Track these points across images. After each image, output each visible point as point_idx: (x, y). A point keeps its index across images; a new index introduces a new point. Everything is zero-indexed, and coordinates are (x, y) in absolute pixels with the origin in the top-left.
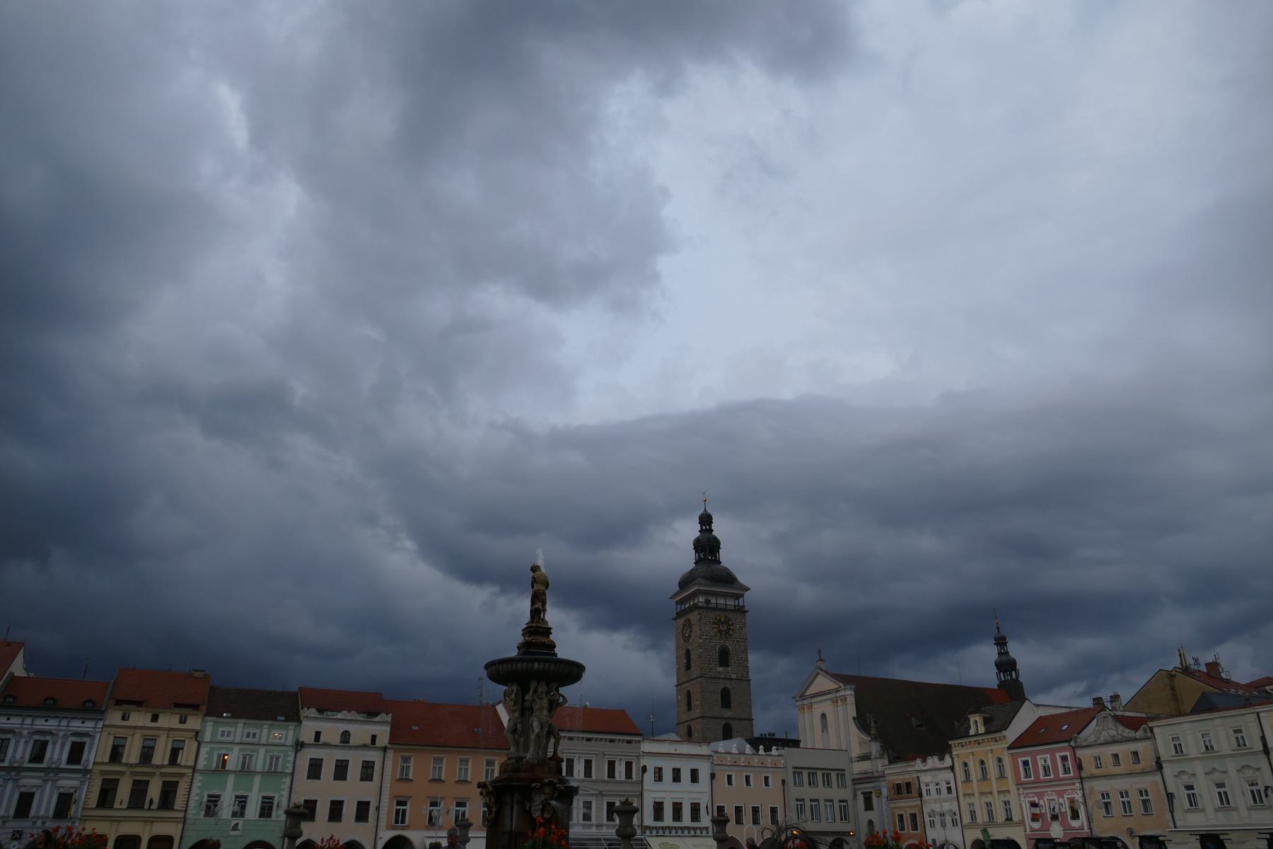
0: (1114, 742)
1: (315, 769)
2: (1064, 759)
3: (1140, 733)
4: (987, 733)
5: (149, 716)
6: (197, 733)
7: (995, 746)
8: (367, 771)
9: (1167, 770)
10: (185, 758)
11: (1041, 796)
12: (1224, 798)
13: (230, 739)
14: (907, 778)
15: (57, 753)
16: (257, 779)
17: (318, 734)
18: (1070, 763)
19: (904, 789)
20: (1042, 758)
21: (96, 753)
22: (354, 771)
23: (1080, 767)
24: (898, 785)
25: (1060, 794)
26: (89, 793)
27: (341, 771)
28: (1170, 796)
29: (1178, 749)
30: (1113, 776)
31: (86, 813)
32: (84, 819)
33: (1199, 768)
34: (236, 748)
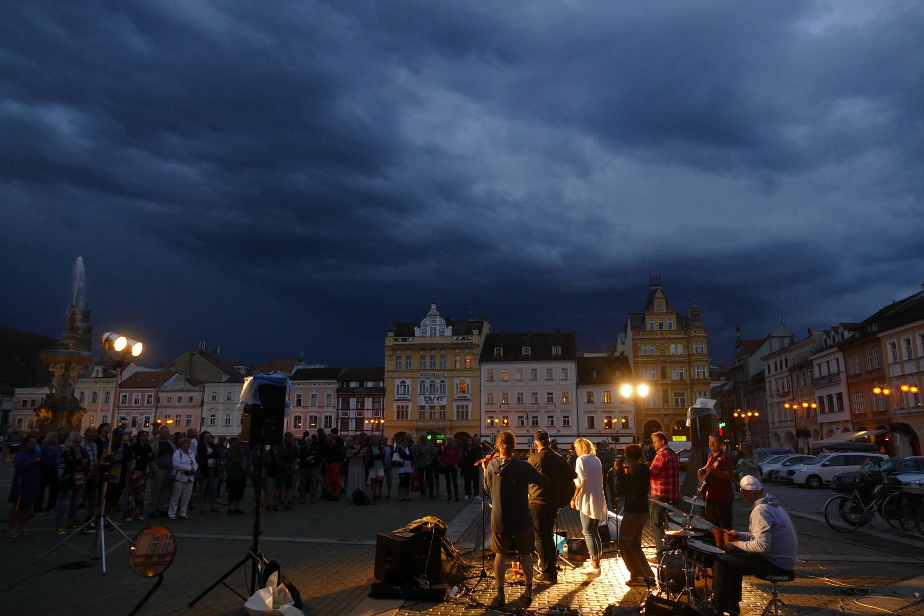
0: (182, 391)
2: (150, 396)
3: (197, 388)
4: (103, 377)
7: (106, 385)
9: (205, 407)
11: (128, 414)
12: (228, 421)
14: (33, 397)
18: (152, 399)
19: (29, 405)
20: (136, 394)
23: (158, 401)
24: (25, 402)
25: (141, 414)
28: (203, 419)
29: (214, 398)
30: (176, 407)
33: (221, 407)
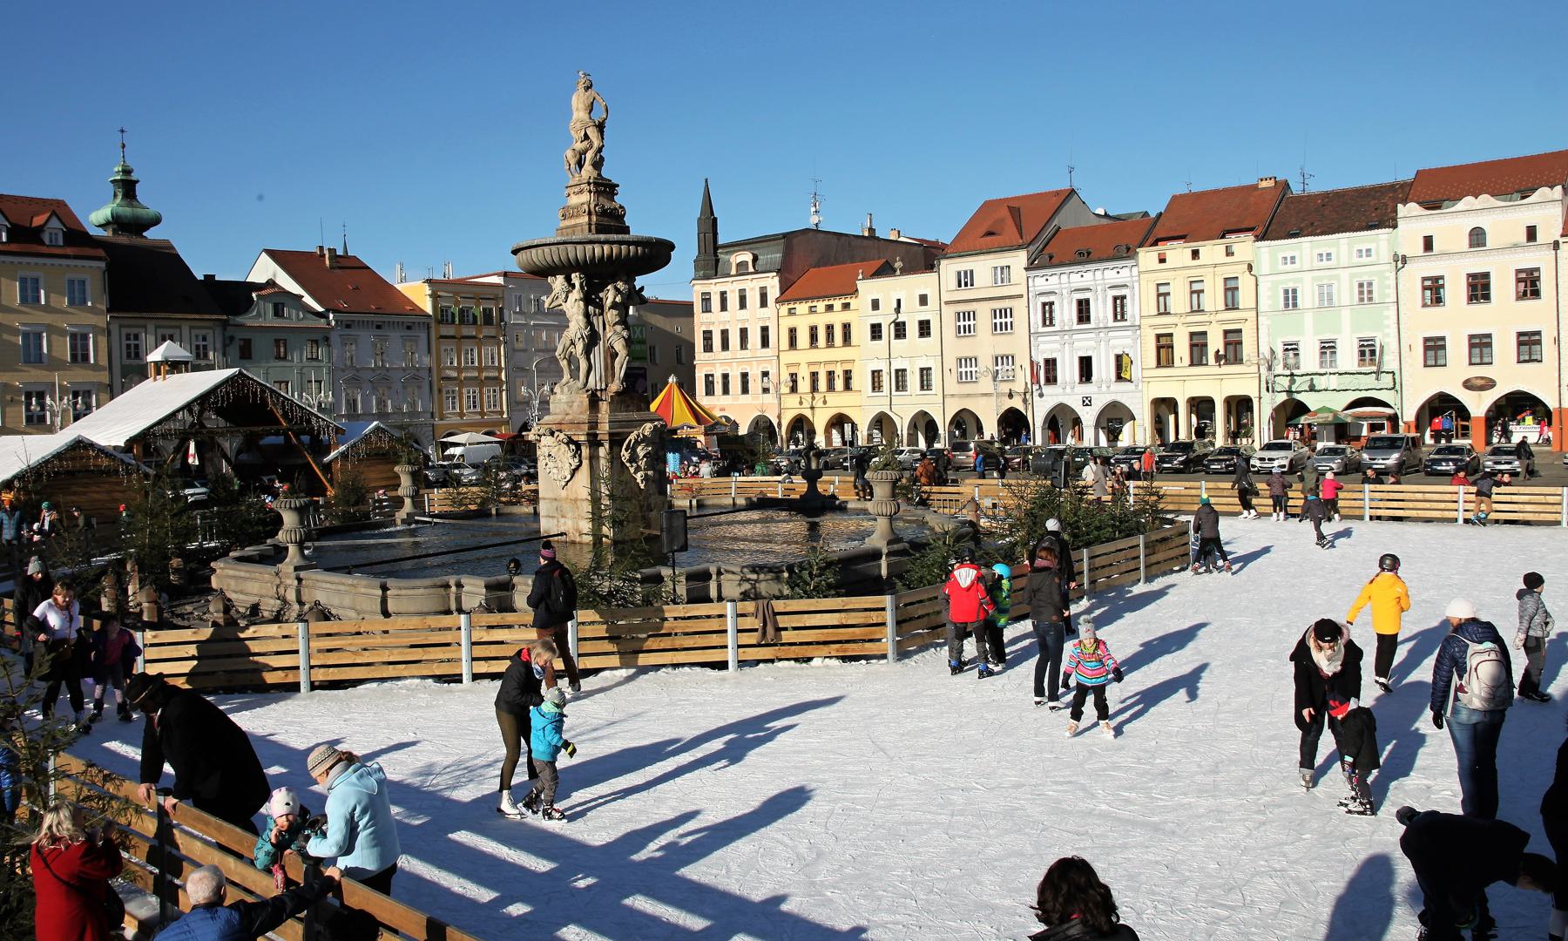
1: (1434, 290)
5: (1188, 252)
6: (1250, 267)
8: (1529, 285)
10: (1245, 297)
13: (1296, 266)
15: (1101, 310)
16: (1346, 313)
17: (1428, 243)
21: (1141, 304)
22: (1503, 286)
26: (1145, 354)
27: (1479, 288)
31: (1146, 373)
32: (1147, 380)
34: (1307, 276)
